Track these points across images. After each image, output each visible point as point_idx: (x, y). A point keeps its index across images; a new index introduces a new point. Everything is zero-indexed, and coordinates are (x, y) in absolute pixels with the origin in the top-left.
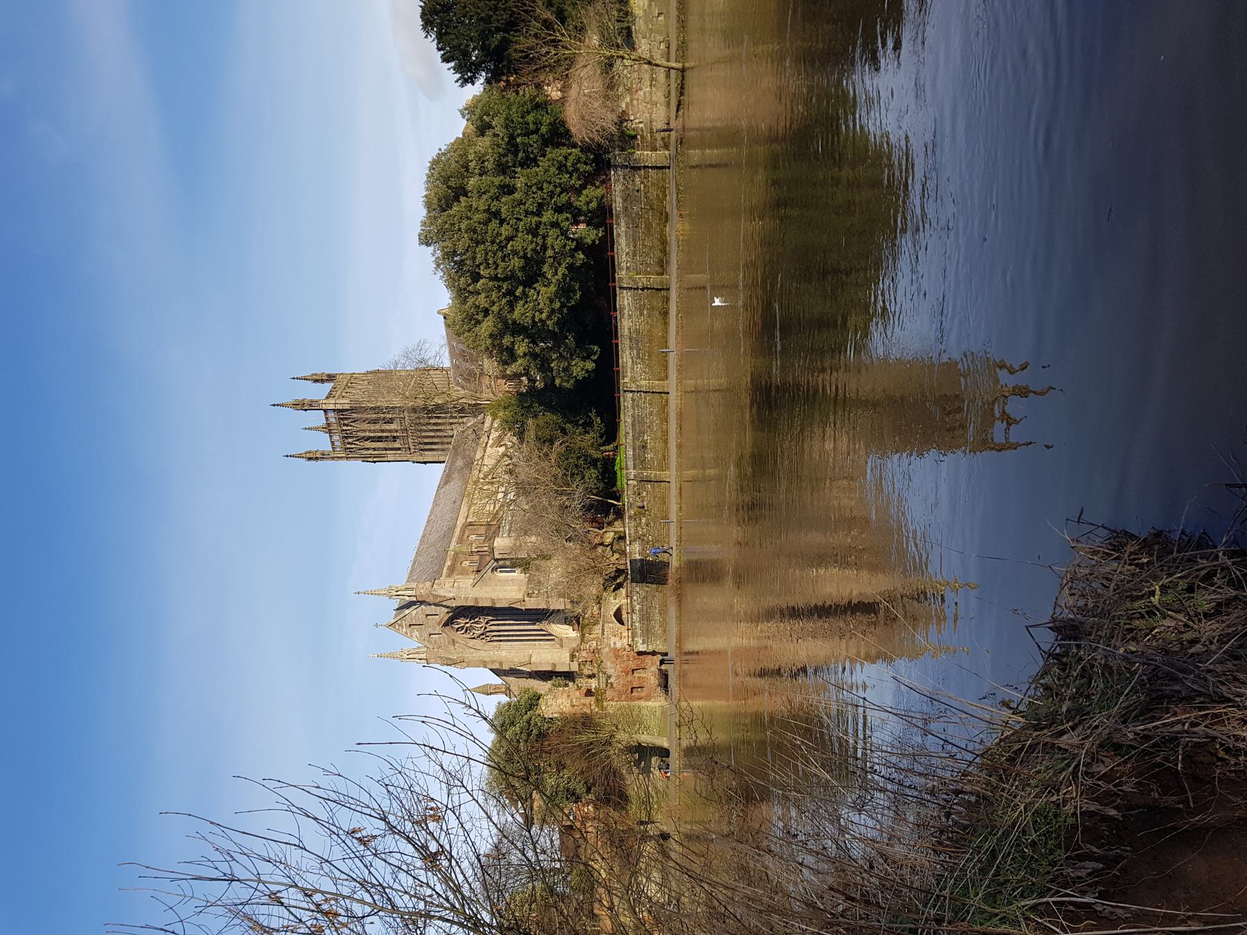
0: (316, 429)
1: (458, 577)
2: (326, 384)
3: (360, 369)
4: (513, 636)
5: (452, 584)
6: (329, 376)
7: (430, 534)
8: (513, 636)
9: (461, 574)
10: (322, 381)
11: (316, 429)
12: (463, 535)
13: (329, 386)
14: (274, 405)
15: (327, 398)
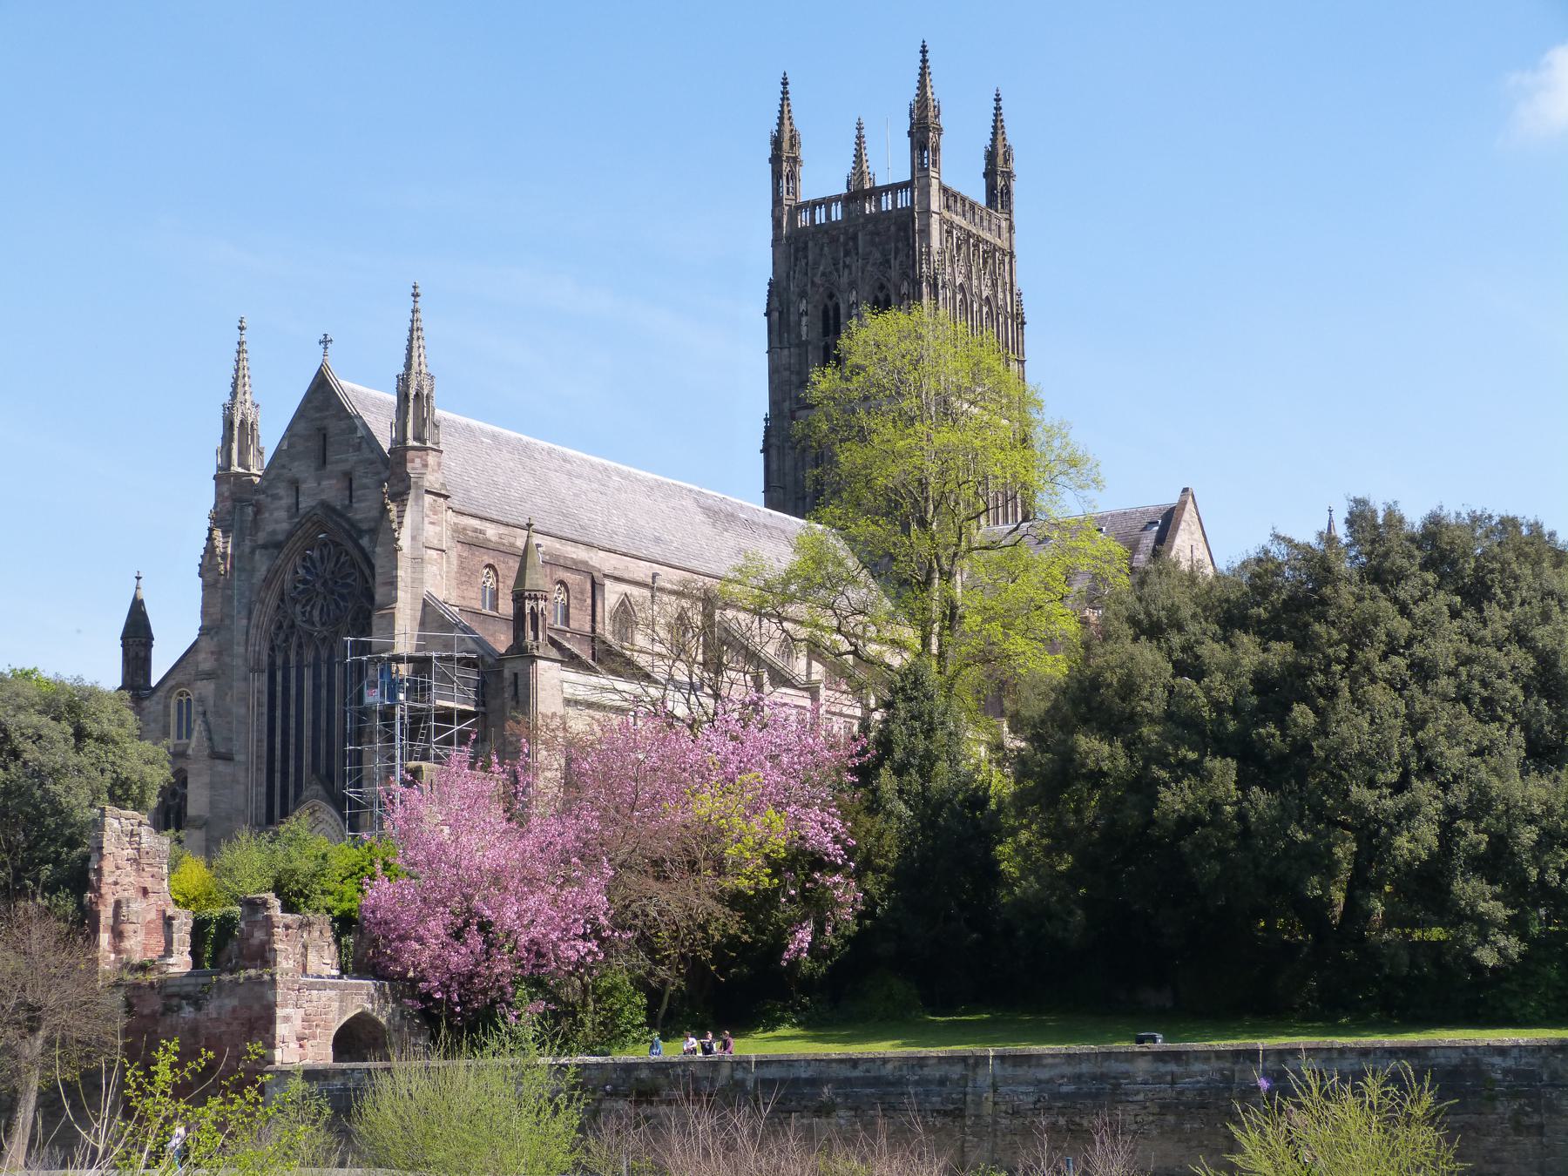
0: (859, 158)
1: (455, 561)
2: (981, 184)
3: (1026, 275)
4: (286, 717)
5: (435, 543)
6: (1007, 192)
7: (569, 474)
8: (286, 717)
9: (462, 567)
10: (990, 174)
11: (859, 158)
12: (566, 568)
13: (977, 193)
14: (924, 51)
15: (945, 190)
